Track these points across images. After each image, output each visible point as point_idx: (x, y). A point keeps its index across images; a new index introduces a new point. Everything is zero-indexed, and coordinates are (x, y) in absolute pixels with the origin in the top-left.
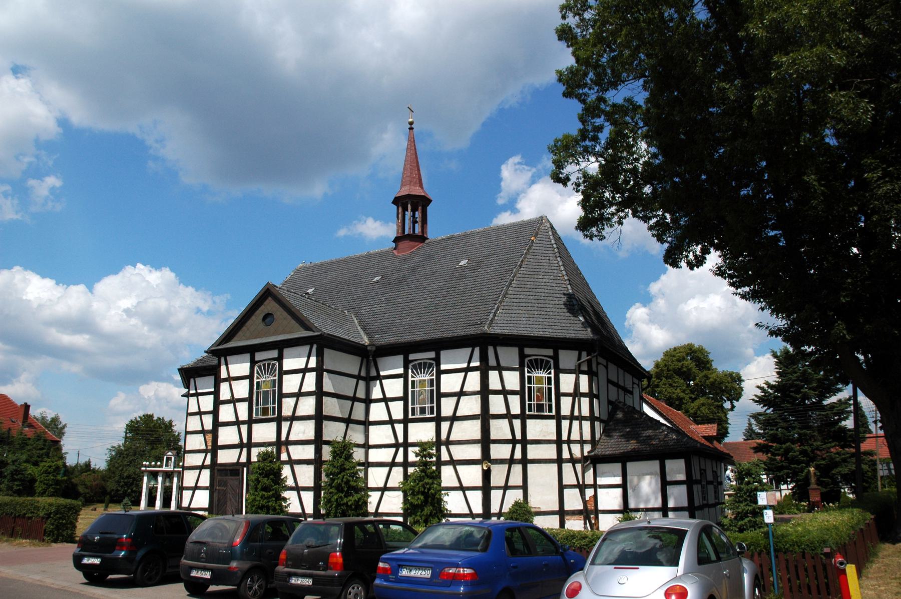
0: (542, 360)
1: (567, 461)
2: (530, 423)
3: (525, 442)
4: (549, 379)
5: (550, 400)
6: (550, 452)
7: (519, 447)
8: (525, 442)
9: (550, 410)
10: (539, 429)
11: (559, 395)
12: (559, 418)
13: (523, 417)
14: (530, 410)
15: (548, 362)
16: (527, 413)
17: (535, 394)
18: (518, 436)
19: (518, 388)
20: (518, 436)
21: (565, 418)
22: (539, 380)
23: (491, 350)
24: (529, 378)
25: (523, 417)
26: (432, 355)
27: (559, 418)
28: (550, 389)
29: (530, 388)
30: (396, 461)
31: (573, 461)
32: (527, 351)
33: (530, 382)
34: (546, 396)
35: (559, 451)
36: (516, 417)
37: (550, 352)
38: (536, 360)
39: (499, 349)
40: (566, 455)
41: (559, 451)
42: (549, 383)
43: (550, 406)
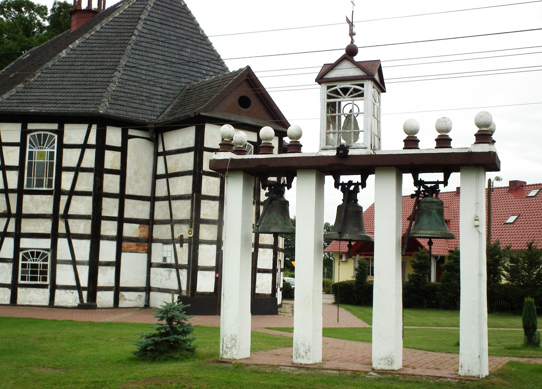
0: (46, 136)
1: (63, 236)
3: (20, 216)
4: (52, 154)
5: (51, 175)
6: (46, 226)
7: (13, 221)
9: (50, 185)
11: (60, 169)
12: (58, 193)
13: (21, 192)
14: (29, 185)
17: (35, 169)
18: (14, 210)
19: (16, 163)
20: (14, 210)
21: (64, 193)
22: (41, 155)
24: (31, 153)
25: (21, 192)
27: (58, 193)
28: (51, 164)
29: (30, 164)
31: (69, 236)
34: (46, 171)
35: (55, 226)
36: (13, 191)
37: (55, 126)
38: (39, 135)
40: (62, 229)
41: (55, 226)
42: (51, 157)
43: (50, 181)
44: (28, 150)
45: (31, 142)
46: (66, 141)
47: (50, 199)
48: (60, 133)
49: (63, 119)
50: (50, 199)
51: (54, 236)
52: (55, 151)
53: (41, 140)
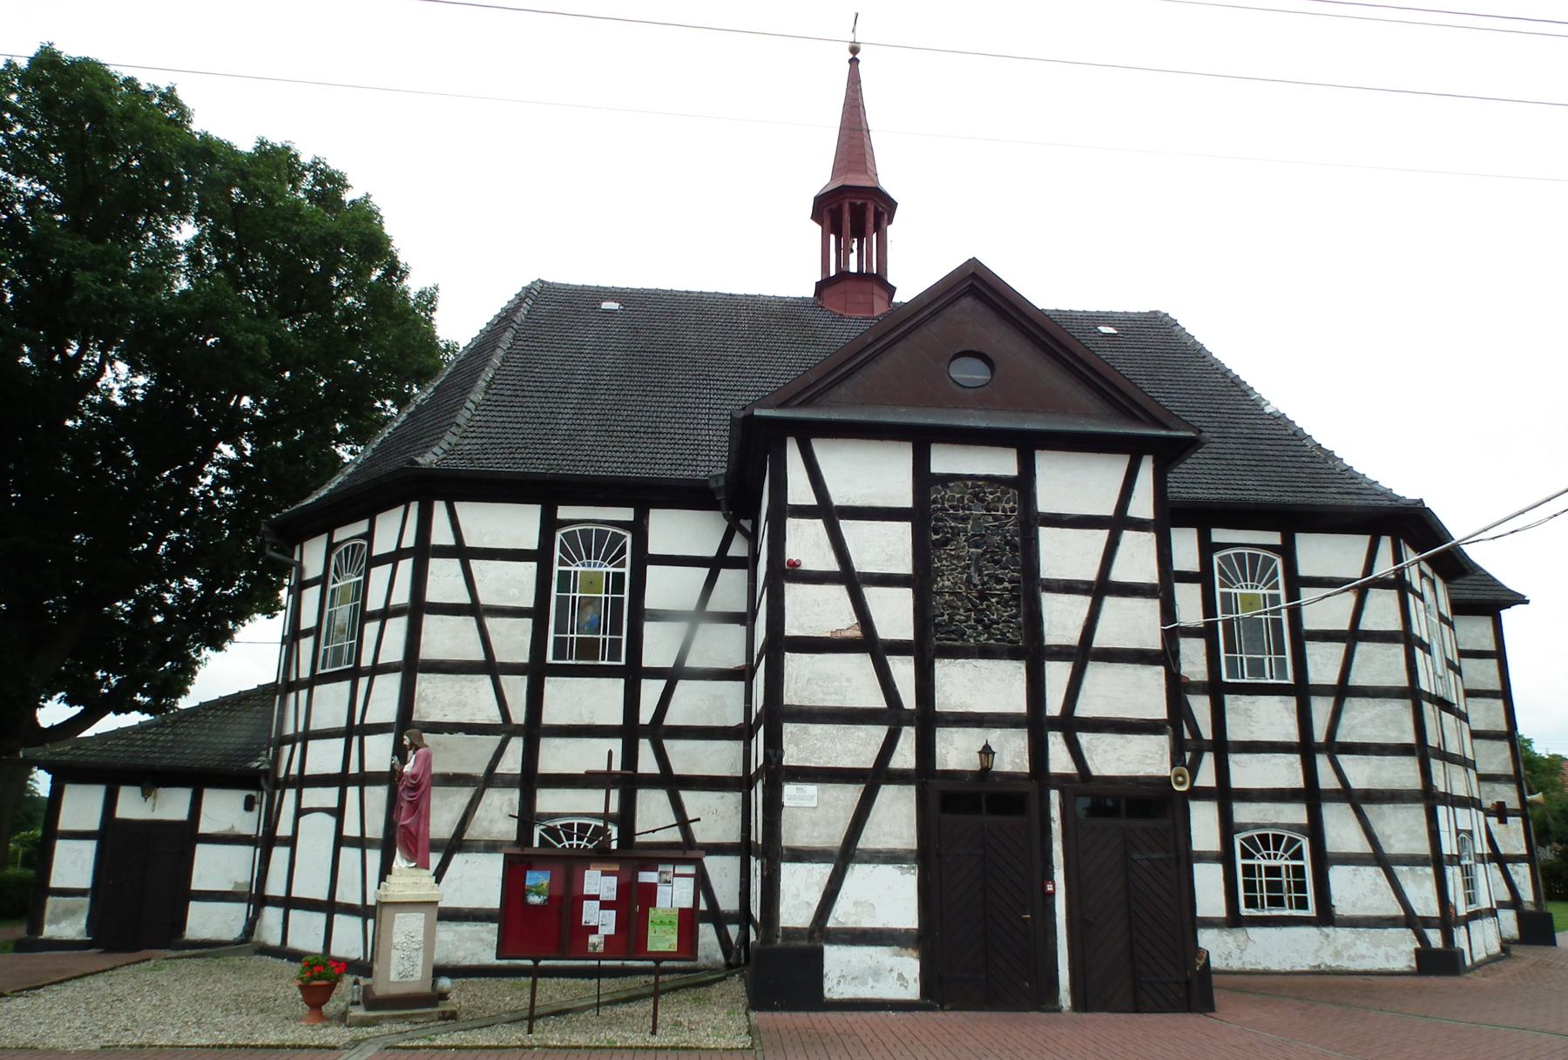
2: (552, 685)
3: (534, 731)
4: (619, 578)
5: (616, 629)
7: (516, 746)
8: (534, 731)
9: (615, 655)
10: (568, 699)
12: (633, 674)
13: (537, 672)
15: (617, 538)
16: (550, 659)
23: (440, 509)
24: (564, 576)
25: (537, 672)
26: (362, 527)
27: (633, 674)
28: (618, 603)
30: (501, 769)
32: (564, 513)
33: (563, 587)
35: (630, 756)
37: (627, 514)
39: (461, 508)
40: (647, 763)
41: (630, 756)
42: (618, 586)
43: (616, 644)
44: (557, 568)
45: (563, 549)
46: (653, 549)
47: (617, 687)
48: (639, 529)
49: (649, 494)
50: (617, 687)
51: (627, 782)
52: (627, 570)
53: (592, 543)
